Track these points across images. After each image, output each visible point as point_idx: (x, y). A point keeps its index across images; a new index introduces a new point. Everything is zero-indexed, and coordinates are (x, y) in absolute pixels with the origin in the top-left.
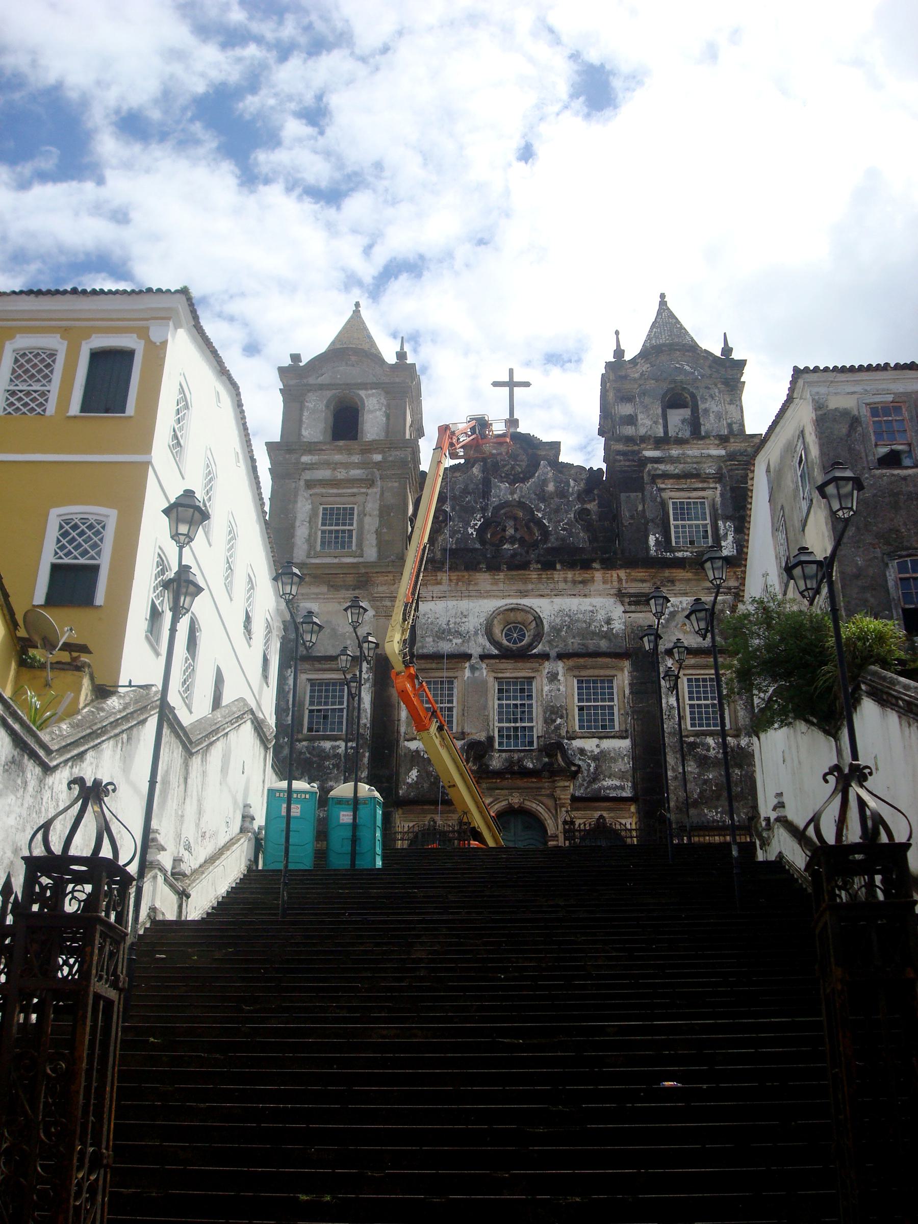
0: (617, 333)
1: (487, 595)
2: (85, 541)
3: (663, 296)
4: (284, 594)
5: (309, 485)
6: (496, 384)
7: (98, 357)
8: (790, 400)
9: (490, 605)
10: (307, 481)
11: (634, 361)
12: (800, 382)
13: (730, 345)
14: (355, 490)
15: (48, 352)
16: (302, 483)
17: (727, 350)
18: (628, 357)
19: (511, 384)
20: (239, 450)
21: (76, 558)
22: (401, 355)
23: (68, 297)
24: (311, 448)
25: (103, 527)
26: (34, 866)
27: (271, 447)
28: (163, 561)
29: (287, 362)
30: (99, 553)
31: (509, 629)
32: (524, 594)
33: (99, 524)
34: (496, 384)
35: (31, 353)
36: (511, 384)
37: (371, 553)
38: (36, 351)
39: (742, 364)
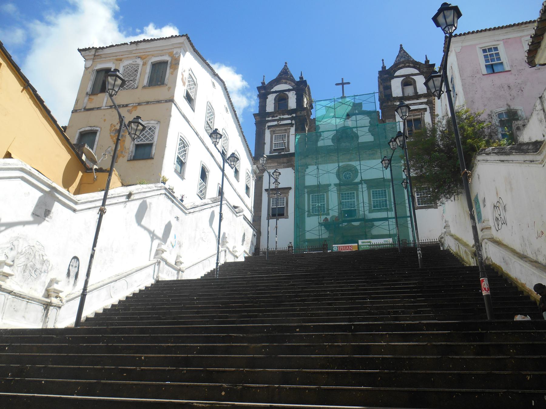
0: (383, 60)
2: (148, 134)
3: (401, 45)
4: (213, 142)
5: (269, 127)
7: (155, 65)
10: (268, 126)
13: (428, 59)
14: (286, 128)
15: (136, 66)
17: (427, 61)
18: (387, 68)
19: (343, 84)
20: (227, 106)
21: (145, 141)
22: (301, 78)
23: (142, 43)
24: (269, 114)
25: (155, 129)
28: (184, 142)
29: (261, 85)
30: (153, 139)
31: (346, 174)
32: (350, 160)
33: (153, 127)
34: (337, 84)
35: (130, 67)
38: (132, 66)
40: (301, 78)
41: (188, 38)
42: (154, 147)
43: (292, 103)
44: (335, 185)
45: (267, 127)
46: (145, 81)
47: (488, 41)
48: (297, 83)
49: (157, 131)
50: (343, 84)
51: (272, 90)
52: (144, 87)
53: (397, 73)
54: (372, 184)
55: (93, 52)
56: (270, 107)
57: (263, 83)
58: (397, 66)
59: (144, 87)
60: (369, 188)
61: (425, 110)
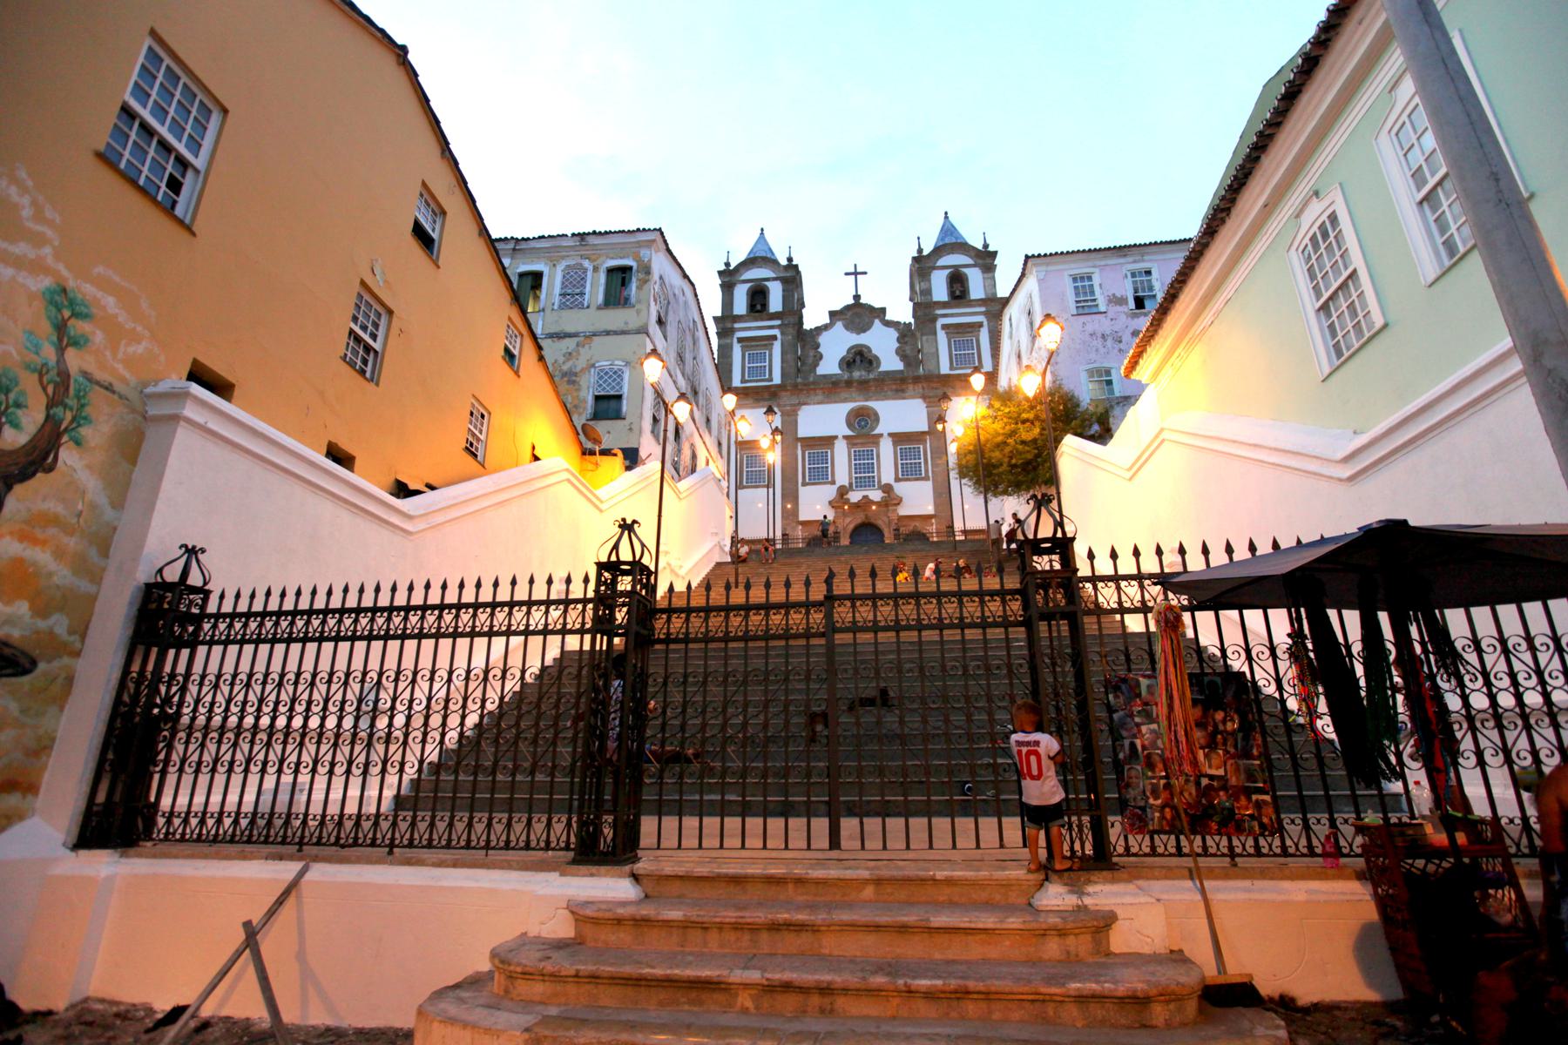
1: (845, 400)
5: (740, 340)
6: (847, 274)
8: (1023, 275)
9: (848, 406)
11: (929, 255)
12: (1029, 264)
16: (735, 340)
17: (986, 246)
18: (925, 253)
22: (790, 259)
24: (739, 318)
26: (601, 566)
27: (715, 318)
29: (723, 268)
34: (847, 274)
36: (856, 274)
37: (777, 380)
39: (995, 253)
40: (790, 259)
41: (662, 233)
42: (625, 402)
43: (775, 303)
44: (845, 437)
45: (735, 340)
46: (600, 298)
47: (1081, 268)
48: (787, 268)
49: (626, 376)
50: (856, 274)
51: (743, 278)
52: (599, 308)
53: (941, 262)
54: (898, 438)
55: (511, 245)
56: (740, 306)
57: (727, 264)
58: (939, 251)
59: (599, 308)
60: (895, 444)
61: (980, 325)
